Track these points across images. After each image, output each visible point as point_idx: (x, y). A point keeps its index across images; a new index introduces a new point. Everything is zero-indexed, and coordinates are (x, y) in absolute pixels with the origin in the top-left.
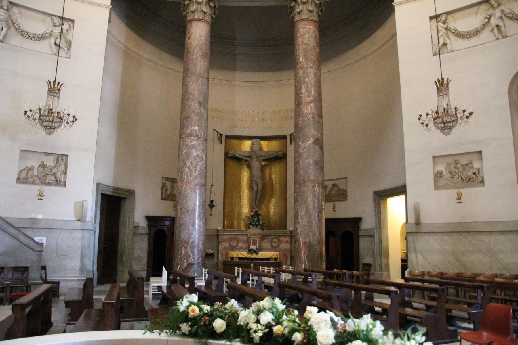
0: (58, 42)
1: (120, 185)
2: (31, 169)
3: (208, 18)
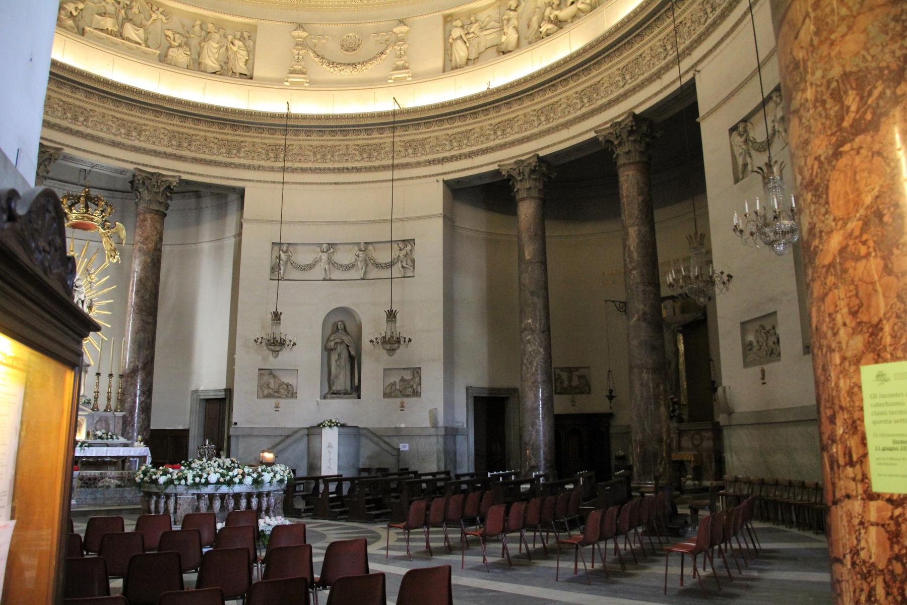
0: (404, 265)
1: (497, 385)
2: (394, 384)
3: (535, 193)
